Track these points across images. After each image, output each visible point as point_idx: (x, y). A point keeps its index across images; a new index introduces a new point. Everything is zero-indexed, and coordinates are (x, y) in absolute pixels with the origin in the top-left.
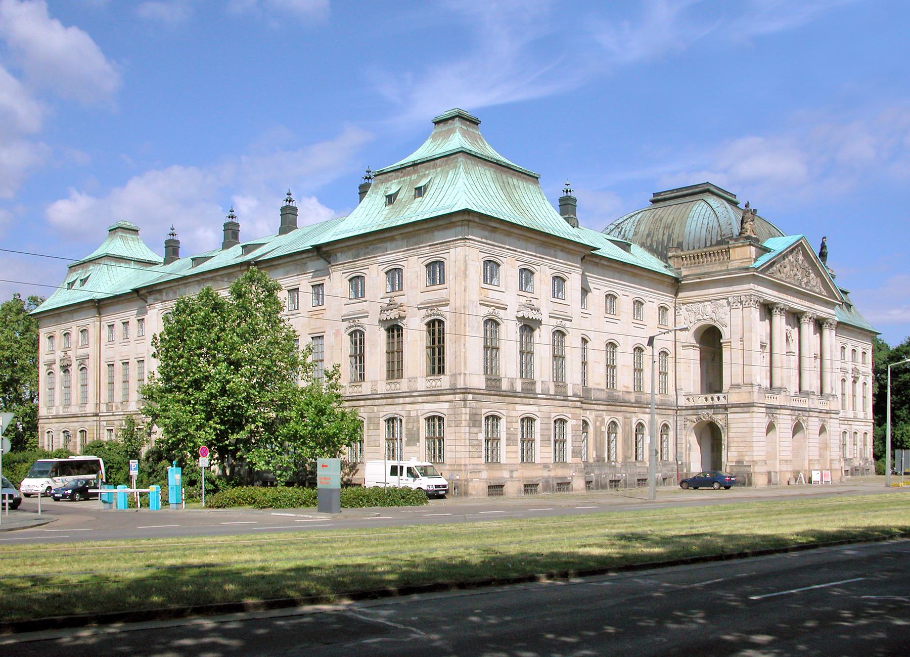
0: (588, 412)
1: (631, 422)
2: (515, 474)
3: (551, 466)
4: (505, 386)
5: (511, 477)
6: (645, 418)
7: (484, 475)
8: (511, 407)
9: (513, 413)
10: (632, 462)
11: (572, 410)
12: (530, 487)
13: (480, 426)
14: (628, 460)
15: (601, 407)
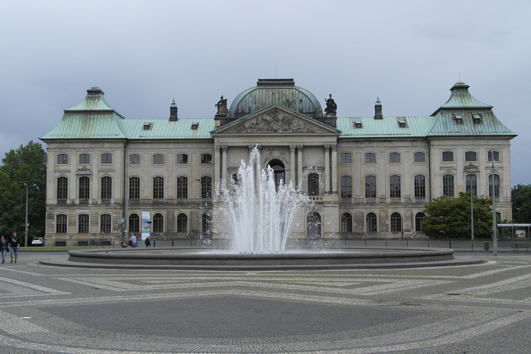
0: (137, 210)
1: (174, 214)
2: (73, 238)
3: (97, 234)
4: (68, 202)
5: (70, 239)
6: (187, 212)
7: (54, 238)
8: (72, 211)
9: (74, 213)
10: (174, 233)
11: (113, 210)
12: (82, 243)
13: (53, 218)
14: (171, 232)
15: (148, 207)
